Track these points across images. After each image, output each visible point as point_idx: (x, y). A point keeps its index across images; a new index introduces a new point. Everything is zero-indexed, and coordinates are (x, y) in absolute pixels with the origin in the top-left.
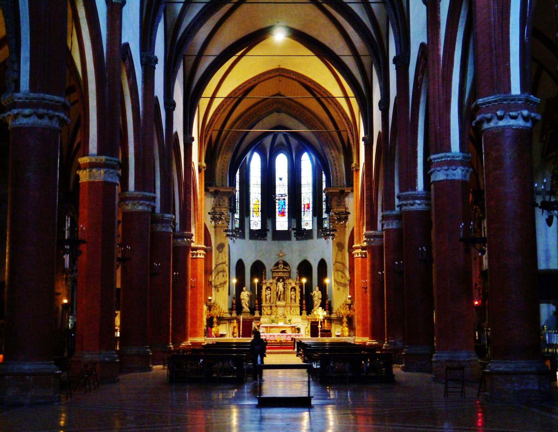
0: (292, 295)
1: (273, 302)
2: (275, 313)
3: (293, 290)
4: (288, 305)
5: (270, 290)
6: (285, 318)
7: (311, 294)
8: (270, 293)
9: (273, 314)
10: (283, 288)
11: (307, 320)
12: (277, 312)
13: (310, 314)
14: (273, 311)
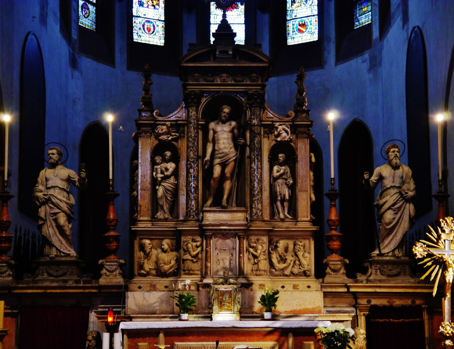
0: (276, 179)
1: (188, 214)
2: (196, 267)
3: (281, 156)
4: (257, 225)
5: (175, 159)
6: (247, 291)
7: (366, 176)
8: (176, 173)
9: (189, 273)
10: (236, 146)
11: (351, 300)
12: (206, 260)
13: (364, 271)
14: (188, 257)
